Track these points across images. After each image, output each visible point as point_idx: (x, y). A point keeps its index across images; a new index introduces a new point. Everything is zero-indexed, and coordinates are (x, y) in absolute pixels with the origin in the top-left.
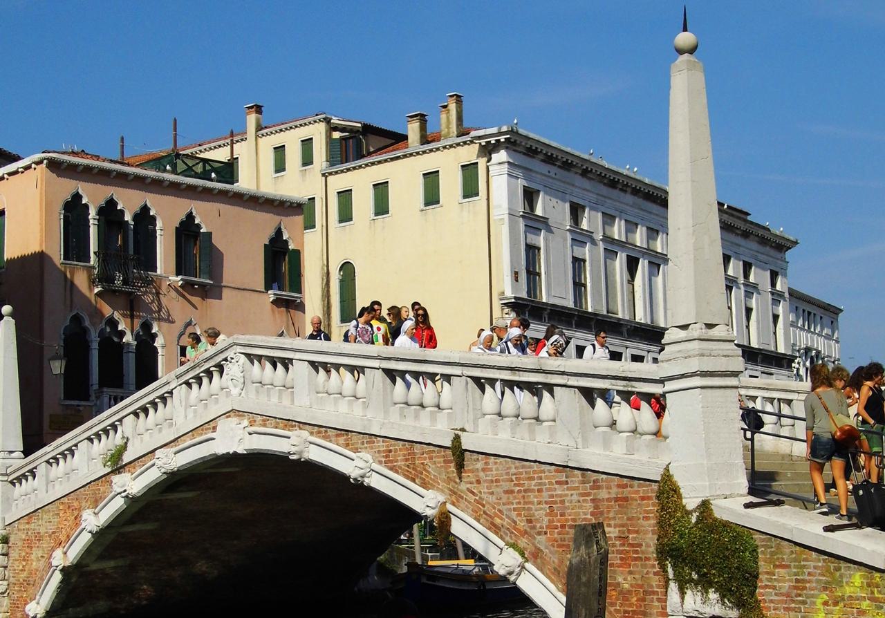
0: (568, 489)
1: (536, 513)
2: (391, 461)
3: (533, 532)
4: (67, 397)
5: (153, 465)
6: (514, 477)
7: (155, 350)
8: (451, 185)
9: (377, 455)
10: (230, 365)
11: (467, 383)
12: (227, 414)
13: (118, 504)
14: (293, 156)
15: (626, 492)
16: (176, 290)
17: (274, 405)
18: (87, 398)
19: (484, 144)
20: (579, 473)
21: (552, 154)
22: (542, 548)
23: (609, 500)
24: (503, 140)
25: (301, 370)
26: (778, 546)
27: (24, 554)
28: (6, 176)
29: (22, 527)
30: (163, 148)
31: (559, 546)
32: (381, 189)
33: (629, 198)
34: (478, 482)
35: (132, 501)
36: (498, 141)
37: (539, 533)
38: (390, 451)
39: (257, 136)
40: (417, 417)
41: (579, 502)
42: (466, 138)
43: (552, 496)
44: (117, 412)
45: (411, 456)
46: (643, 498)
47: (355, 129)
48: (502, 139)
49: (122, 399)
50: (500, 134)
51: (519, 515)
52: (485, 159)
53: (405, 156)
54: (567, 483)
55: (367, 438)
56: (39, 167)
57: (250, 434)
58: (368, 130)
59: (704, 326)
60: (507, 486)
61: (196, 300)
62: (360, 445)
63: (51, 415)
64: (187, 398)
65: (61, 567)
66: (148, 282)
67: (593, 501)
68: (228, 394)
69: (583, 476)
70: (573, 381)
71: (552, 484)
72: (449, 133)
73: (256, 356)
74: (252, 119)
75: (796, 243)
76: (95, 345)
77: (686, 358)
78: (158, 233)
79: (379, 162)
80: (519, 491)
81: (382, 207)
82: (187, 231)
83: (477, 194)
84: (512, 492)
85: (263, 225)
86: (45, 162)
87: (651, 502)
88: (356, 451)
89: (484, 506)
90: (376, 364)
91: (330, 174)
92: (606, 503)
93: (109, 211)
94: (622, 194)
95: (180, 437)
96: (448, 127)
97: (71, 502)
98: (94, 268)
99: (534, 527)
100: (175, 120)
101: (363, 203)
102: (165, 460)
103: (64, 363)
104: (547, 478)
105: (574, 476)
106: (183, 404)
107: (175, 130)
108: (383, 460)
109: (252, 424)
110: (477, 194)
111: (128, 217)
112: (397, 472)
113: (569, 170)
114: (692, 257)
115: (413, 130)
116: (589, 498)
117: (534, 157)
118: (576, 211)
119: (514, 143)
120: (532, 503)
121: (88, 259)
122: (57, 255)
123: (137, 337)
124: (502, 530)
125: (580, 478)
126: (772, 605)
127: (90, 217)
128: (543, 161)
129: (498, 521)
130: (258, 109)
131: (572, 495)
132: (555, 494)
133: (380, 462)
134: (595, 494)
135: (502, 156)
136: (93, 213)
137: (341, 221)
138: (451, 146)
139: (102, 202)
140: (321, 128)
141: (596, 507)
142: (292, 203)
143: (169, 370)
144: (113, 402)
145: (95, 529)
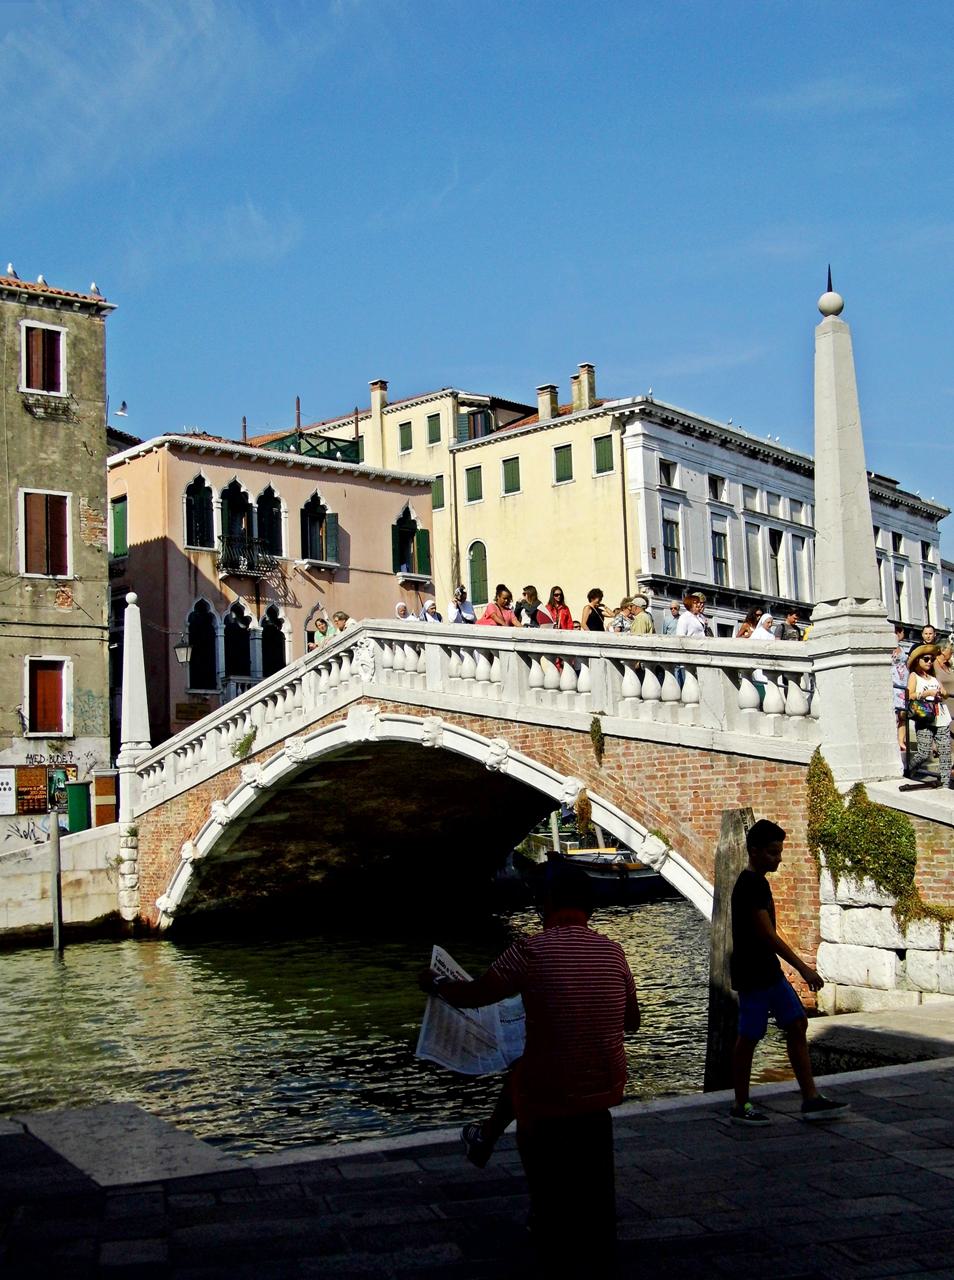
0: (713, 774)
1: (680, 799)
2: (528, 747)
3: (677, 818)
4: (193, 686)
5: (283, 754)
6: (656, 762)
7: (281, 637)
8: (584, 459)
9: (513, 741)
10: (360, 650)
11: (606, 664)
12: (358, 701)
13: (248, 795)
14: (420, 433)
15: (775, 776)
16: (303, 574)
17: (405, 690)
18: (213, 686)
19: (617, 415)
20: (725, 756)
21: (689, 425)
22: (687, 835)
23: (756, 784)
24: (637, 411)
25: (433, 653)
26: (937, 831)
27: (153, 847)
28: (127, 460)
29: (150, 819)
30: (287, 428)
31: (706, 833)
32: (511, 465)
33: (771, 469)
34: (619, 767)
35: (262, 791)
36: (632, 412)
37: (684, 820)
38: (527, 737)
40: (554, 701)
41: (725, 786)
42: (599, 410)
43: (697, 781)
44: (245, 701)
45: (548, 742)
46: (792, 782)
47: (483, 404)
48: (637, 410)
49: (249, 687)
50: (635, 404)
51: (663, 801)
52: (619, 431)
53: (535, 430)
54: (712, 767)
55: (502, 724)
56: (160, 450)
57: (382, 721)
58: (497, 404)
59: (854, 601)
60: (649, 771)
61: (322, 583)
62: (495, 731)
63: (177, 705)
64: (316, 685)
65: (191, 860)
66: (273, 566)
67: (739, 785)
68: (359, 680)
69: (728, 759)
70: (717, 661)
71: (696, 768)
72: (580, 405)
73: (385, 639)
74: (376, 395)
75: (949, 512)
76: (221, 632)
77: (836, 635)
78: (283, 515)
79: (509, 437)
80: (662, 777)
81: (512, 484)
82: (313, 513)
83: (611, 468)
84: (653, 777)
85: (392, 504)
86: (167, 444)
87: (800, 786)
88: (491, 736)
89: (625, 792)
90: (510, 646)
91: (459, 450)
92: (753, 788)
93: (233, 494)
94: (763, 465)
95: (309, 725)
96: (580, 399)
97: (201, 793)
98: (218, 552)
99: (678, 814)
100: (298, 398)
101: (493, 480)
102: (295, 749)
103: (190, 650)
104: (691, 762)
105: (719, 760)
106: (313, 690)
107: (298, 409)
108: (520, 745)
109: (384, 710)
110: (611, 468)
111: (252, 500)
112: (534, 758)
113: (707, 441)
114: (841, 529)
115: (543, 403)
116: (735, 783)
117: (670, 428)
118: (715, 483)
119: (649, 414)
120: (676, 788)
121: (210, 543)
122: (180, 539)
123: (264, 623)
124: (645, 817)
125: (726, 762)
126: (931, 892)
127: (213, 501)
128: (679, 432)
129: (640, 808)
130: (383, 385)
131: (717, 780)
132: (699, 778)
133: (517, 748)
134: (741, 779)
135: (636, 427)
136: (216, 497)
137: (470, 499)
138: (583, 419)
139: (225, 485)
140: (449, 402)
141: (743, 792)
142: (419, 482)
143: (297, 656)
144: (240, 690)
145: (225, 821)
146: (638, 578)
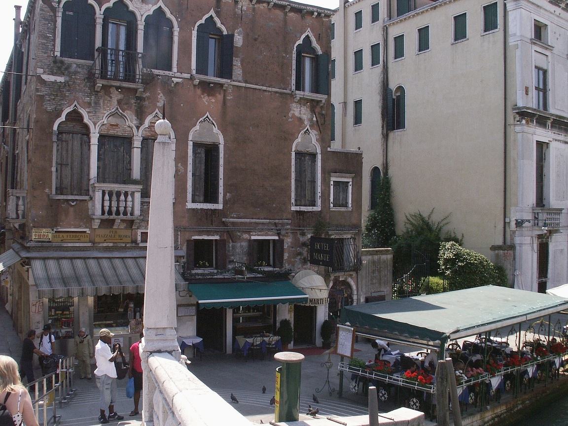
8: (475, 22)
32: (423, 33)
39: (345, 7)
81: (423, 44)
101: (411, 43)
146: (514, 109)
